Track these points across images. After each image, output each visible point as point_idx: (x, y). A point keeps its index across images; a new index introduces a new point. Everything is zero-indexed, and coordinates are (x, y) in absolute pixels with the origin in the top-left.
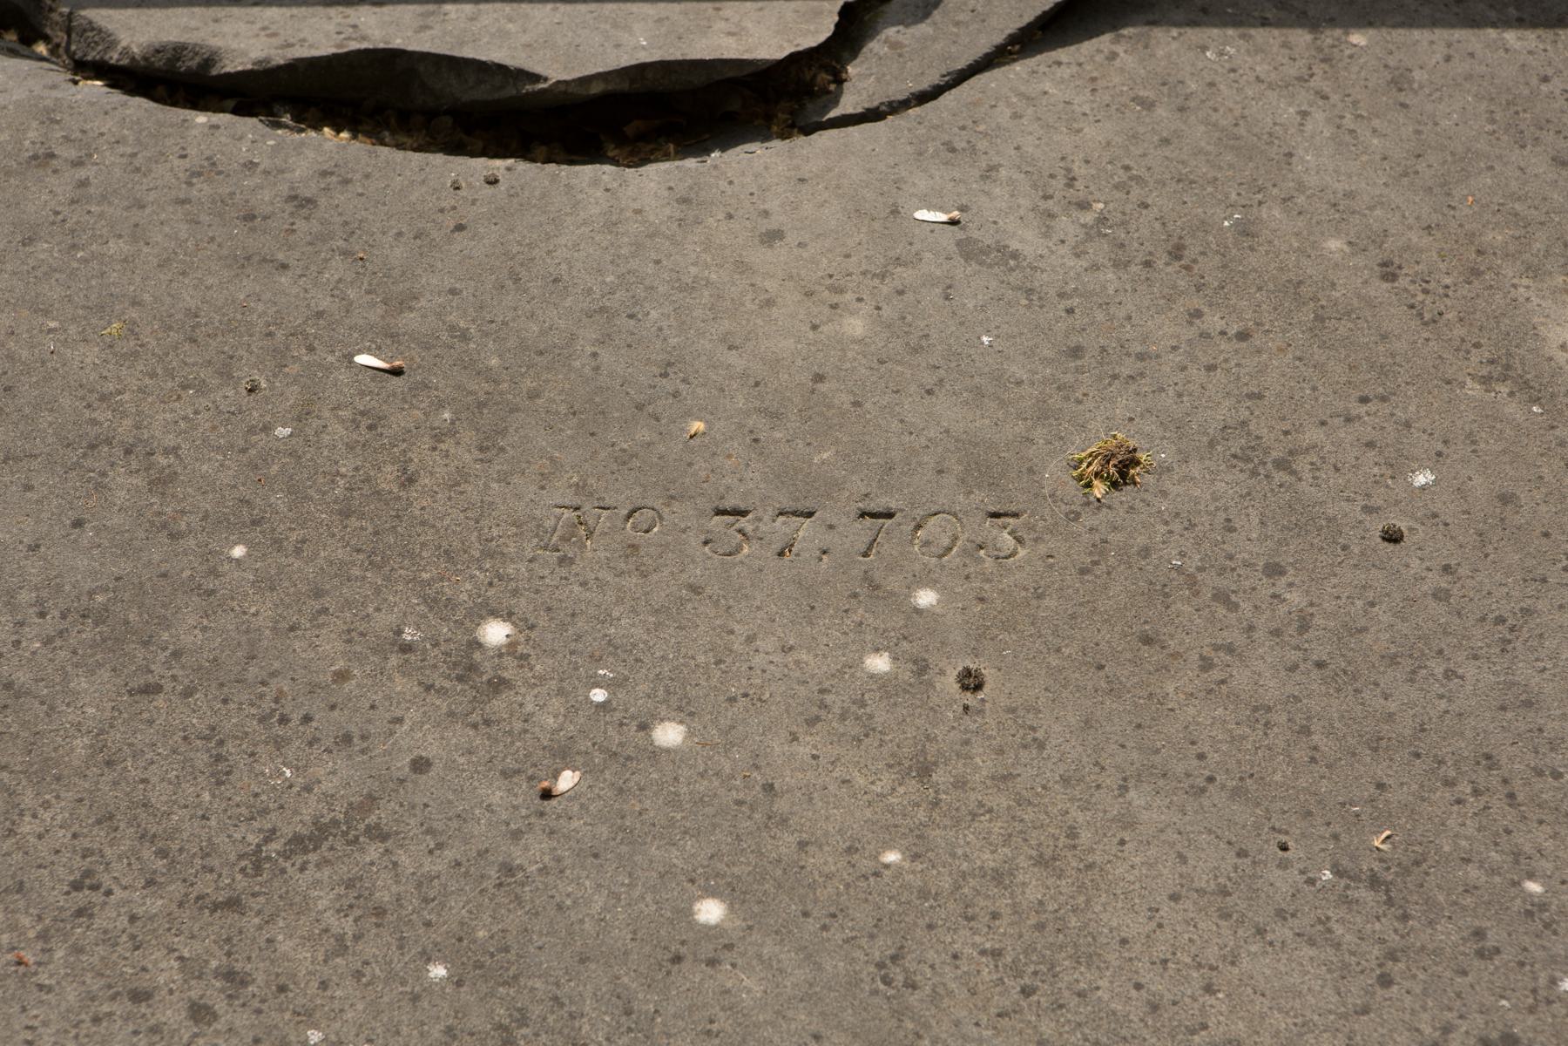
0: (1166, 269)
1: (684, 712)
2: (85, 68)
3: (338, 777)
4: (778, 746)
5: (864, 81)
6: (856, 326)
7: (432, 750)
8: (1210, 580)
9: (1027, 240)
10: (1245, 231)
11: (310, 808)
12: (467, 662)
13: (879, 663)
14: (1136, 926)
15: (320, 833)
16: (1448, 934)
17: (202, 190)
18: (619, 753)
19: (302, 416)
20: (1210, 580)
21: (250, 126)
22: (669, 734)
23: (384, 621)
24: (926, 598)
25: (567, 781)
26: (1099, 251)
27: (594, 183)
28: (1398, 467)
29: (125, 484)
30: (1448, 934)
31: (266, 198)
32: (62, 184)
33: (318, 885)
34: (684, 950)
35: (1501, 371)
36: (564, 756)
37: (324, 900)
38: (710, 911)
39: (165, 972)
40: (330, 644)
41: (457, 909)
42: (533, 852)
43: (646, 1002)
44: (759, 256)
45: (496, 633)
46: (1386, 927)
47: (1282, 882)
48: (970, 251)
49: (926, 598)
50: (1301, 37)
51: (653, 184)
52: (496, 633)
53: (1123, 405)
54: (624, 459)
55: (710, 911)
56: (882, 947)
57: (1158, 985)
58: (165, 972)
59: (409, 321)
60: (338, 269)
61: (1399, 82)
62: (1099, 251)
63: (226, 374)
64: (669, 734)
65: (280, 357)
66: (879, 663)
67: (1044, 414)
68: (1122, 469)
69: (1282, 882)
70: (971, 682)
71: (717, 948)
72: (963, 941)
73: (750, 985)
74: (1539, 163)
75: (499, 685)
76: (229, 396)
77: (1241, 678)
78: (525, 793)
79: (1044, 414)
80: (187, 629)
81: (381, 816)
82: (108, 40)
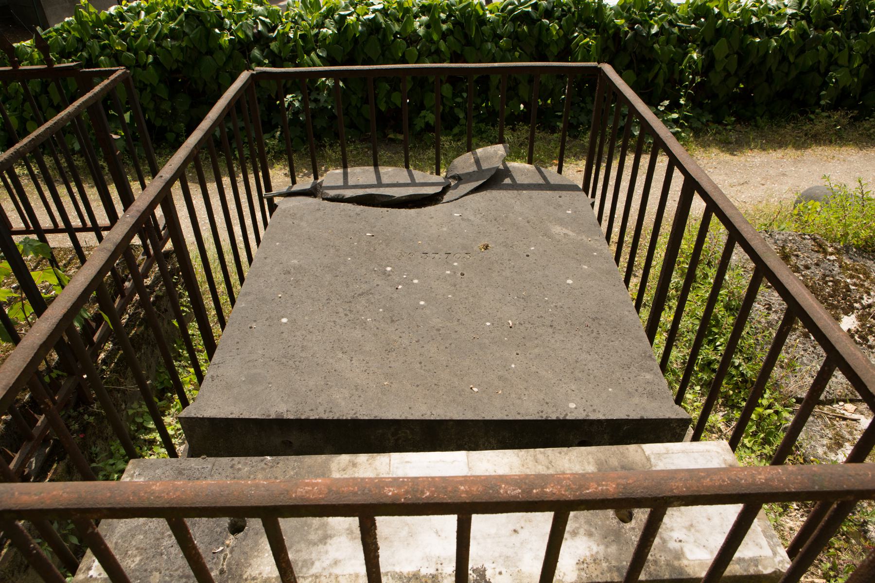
0: (494, 222)
1: (417, 278)
2: (324, 199)
3: (365, 287)
4: (432, 283)
5: (446, 198)
6: (445, 229)
7: (379, 283)
8: (500, 262)
9: (472, 218)
10: (506, 217)
11: (361, 291)
12: (385, 273)
13: (448, 272)
14: (487, 304)
15: (363, 294)
16: (533, 304)
17: (343, 213)
18: (408, 283)
19: (358, 242)
20: (500, 262)
21: (350, 205)
22: (416, 281)
23: (371, 268)
24: (456, 264)
25: (400, 287)
26: (483, 219)
27: (403, 211)
28: (529, 247)
29: (332, 251)
30: (533, 304)
31: (352, 214)
32: (321, 213)
33: (363, 300)
34: (418, 308)
35: (545, 235)
36: (400, 284)
37: (363, 302)
38: (422, 303)
39: (341, 310)
40: (363, 270)
41: (384, 303)
42: (395, 296)
43: (412, 314)
44: (430, 220)
45: (389, 269)
46: (525, 304)
47: (509, 299)
48: (463, 219)
49: (456, 264)
50: (516, 192)
51: (413, 211)
52: (389, 269)
53: (487, 239)
54: (408, 247)
55: (422, 303)
56: (448, 307)
57: (490, 311)
58: (341, 310)
59: (375, 229)
60: (364, 223)
61: (531, 197)
62: (483, 219)
63: (347, 236)
64: (416, 281)
65: (355, 234)
66: (448, 272)
67: (474, 240)
68: (486, 247)
69: (509, 299)
70: (462, 274)
71: (423, 307)
72: (461, 306)
73: (428, 312)
74: (552, 208)
75: (389, 275)
76: (348, 239)
77: (504, 274)
78: (394, 289)
79: (474, 240)
80: (342, 268)
81: (372, 291)
82: (328, 194)
